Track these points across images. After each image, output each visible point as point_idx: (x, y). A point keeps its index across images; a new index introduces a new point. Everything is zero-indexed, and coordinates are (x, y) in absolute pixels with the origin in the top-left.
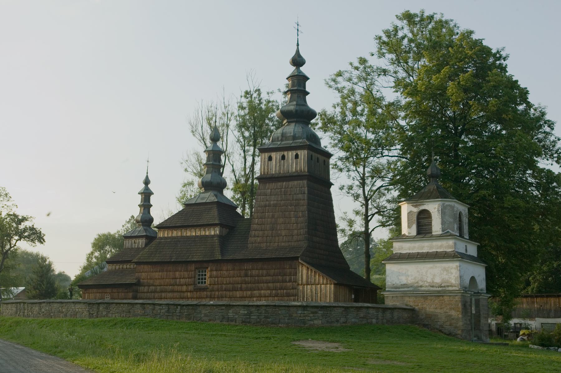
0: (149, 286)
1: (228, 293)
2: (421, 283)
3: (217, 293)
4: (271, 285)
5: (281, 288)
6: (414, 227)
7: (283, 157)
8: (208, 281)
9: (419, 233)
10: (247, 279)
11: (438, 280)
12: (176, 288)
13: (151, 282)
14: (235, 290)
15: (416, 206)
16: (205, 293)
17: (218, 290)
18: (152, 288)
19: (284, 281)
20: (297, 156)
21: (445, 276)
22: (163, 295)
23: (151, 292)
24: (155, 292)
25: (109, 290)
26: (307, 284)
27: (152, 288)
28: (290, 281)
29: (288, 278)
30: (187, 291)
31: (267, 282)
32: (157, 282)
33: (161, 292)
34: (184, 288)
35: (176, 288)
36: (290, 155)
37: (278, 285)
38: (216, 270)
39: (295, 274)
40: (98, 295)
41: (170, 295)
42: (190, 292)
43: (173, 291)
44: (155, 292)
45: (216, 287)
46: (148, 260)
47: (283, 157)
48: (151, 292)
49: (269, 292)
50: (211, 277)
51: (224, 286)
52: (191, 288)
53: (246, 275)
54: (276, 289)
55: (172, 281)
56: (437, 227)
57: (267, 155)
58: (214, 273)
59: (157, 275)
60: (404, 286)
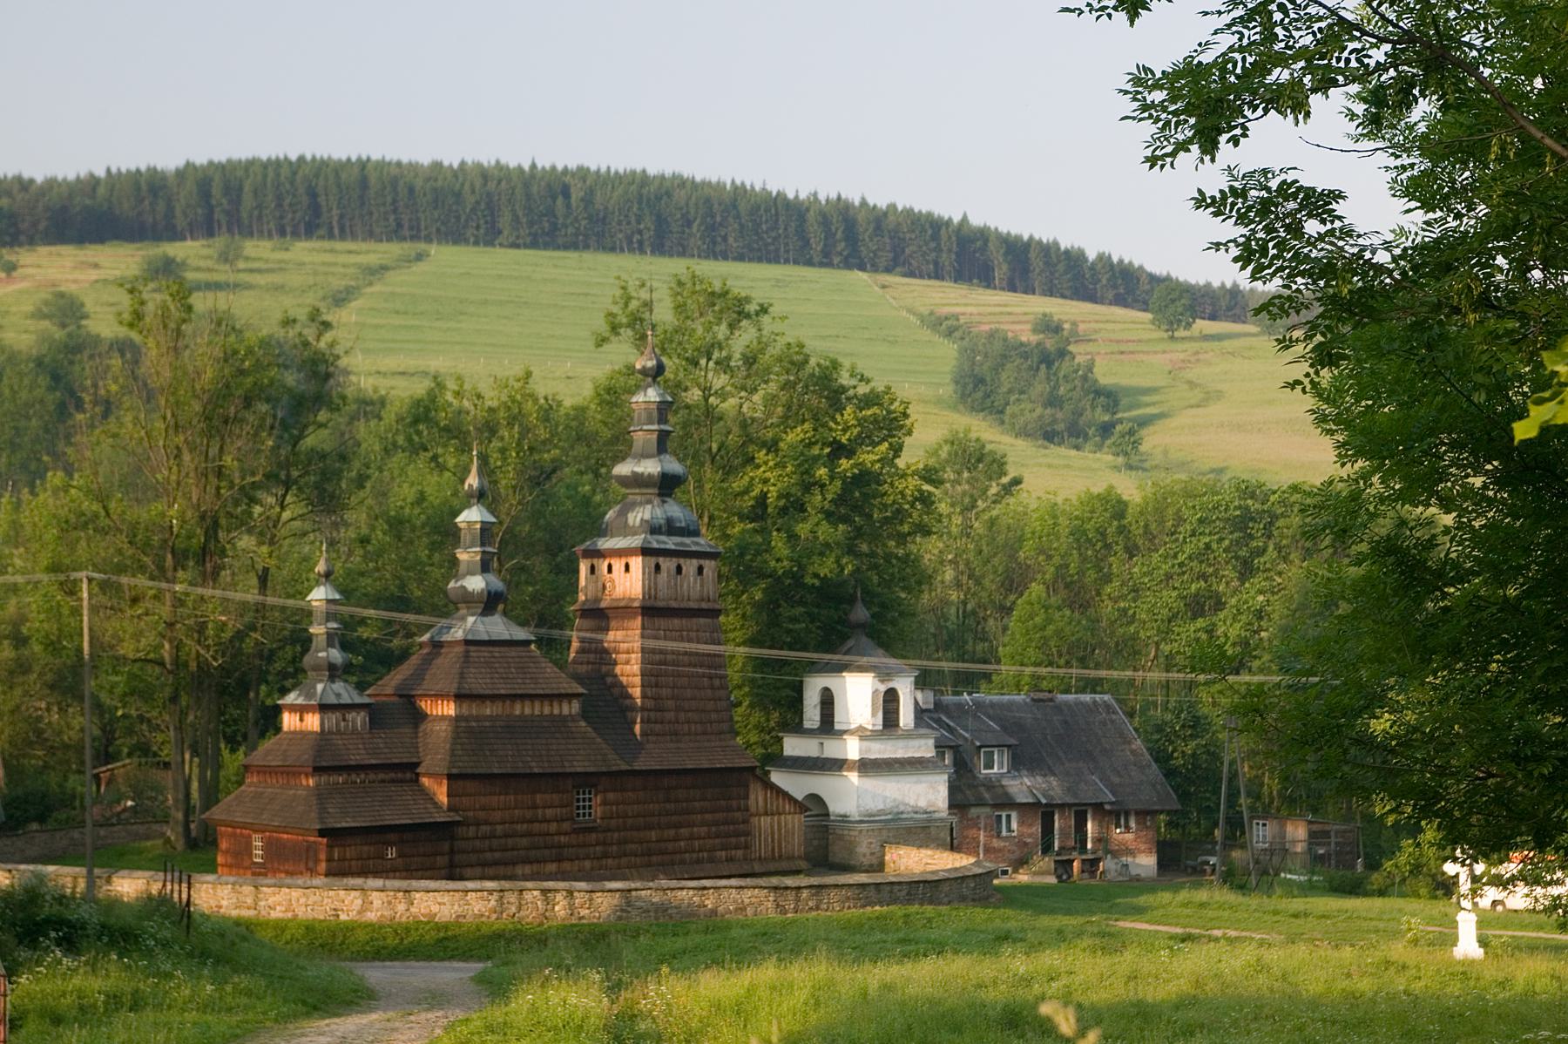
0: (478, 825)
1: (635, 834)
2: (902, 808)
3: (616, 835)
4: (707, 816)
5: (726, 823)
6: (880, 715)
7: (679, 569)
8: (598, 811)
9: (885, 726)
10: (668, 806)
11: (922, 804)
12: (536, 827)
13: (482, 815)
14: (650, 827)
15: (882, 681)
16: (594, 835)
17: (618, 829)
18: (485, 829)
19: (729, 809)
20: (700, 570)
21: (931, 797)
22: (510, 841)
23: (484, 838)
24: (493, 836)
25: (392, 837)
26: (766, 814)
27: (485, 829)
28: (739, 809)
29: (734, 803)
30: (560, 834)
31: (703, 811)
32: (498, 815)
33: (506, 836)
34: (553, 827)
35: (536, 827)
36: (690, 566)
37: (720, 816)
38: (614, 790)
39: (747, 797)
40: (366, 848)
41: (524, 841)
42: (566, 834)
43: (529, 834)
44: (493, 836)
45: (613, 822)
46: (476, 771)
47: (679, 569)
48: (484, 838)
49: (705, 829)
50: (604, 803)
51: (630, 821)
52: (566, 826)
53: (669, 801)
54: (716, 824)
55: (529, 814)
56: (906, 717)
57: (652, 561)
58: (611, 796)
59: (494, 800)
60: (881, 812)
